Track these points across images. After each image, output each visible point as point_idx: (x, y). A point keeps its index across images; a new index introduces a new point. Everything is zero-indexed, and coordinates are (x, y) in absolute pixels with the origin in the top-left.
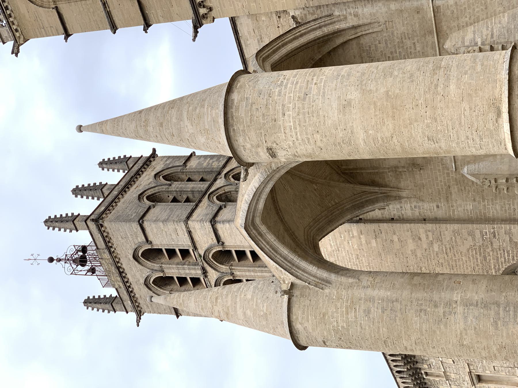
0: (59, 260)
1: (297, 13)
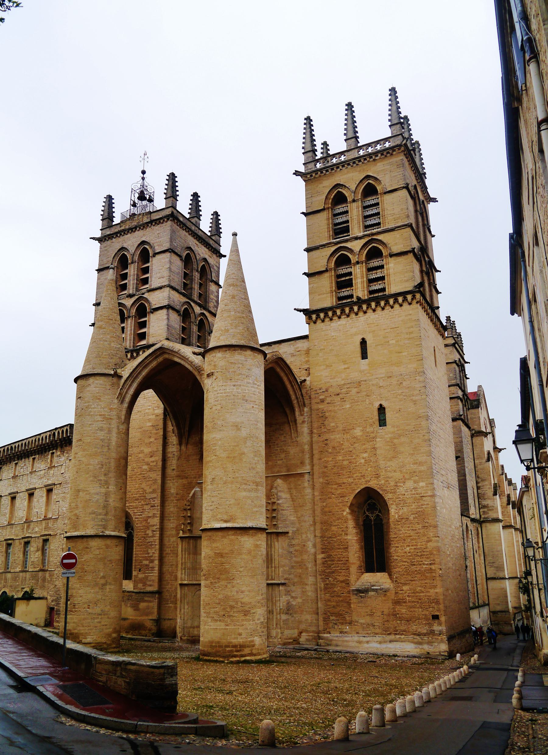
0: (143, 179)
1: (308, 383)
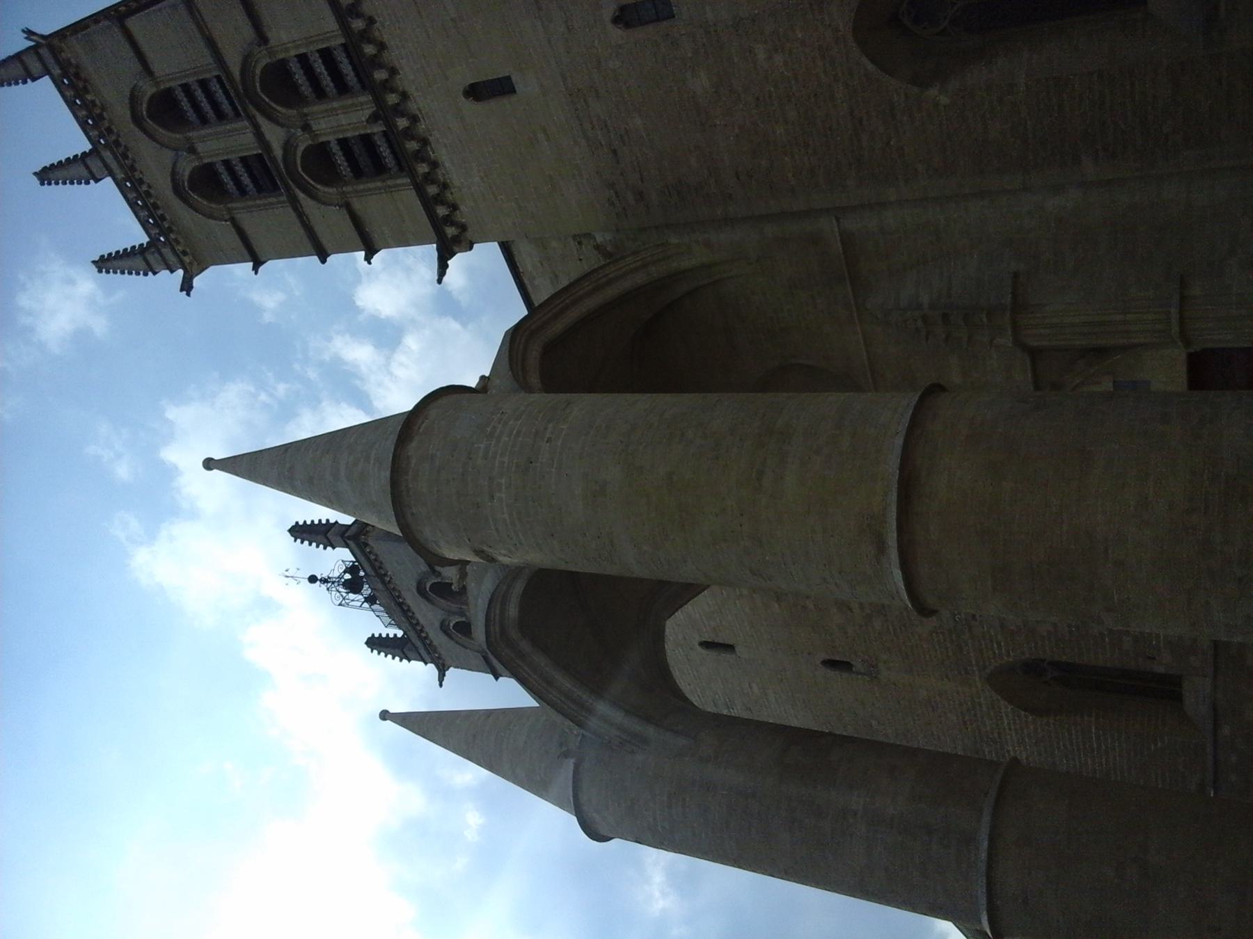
0: (324, 581)
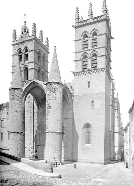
0: (25, 24)
